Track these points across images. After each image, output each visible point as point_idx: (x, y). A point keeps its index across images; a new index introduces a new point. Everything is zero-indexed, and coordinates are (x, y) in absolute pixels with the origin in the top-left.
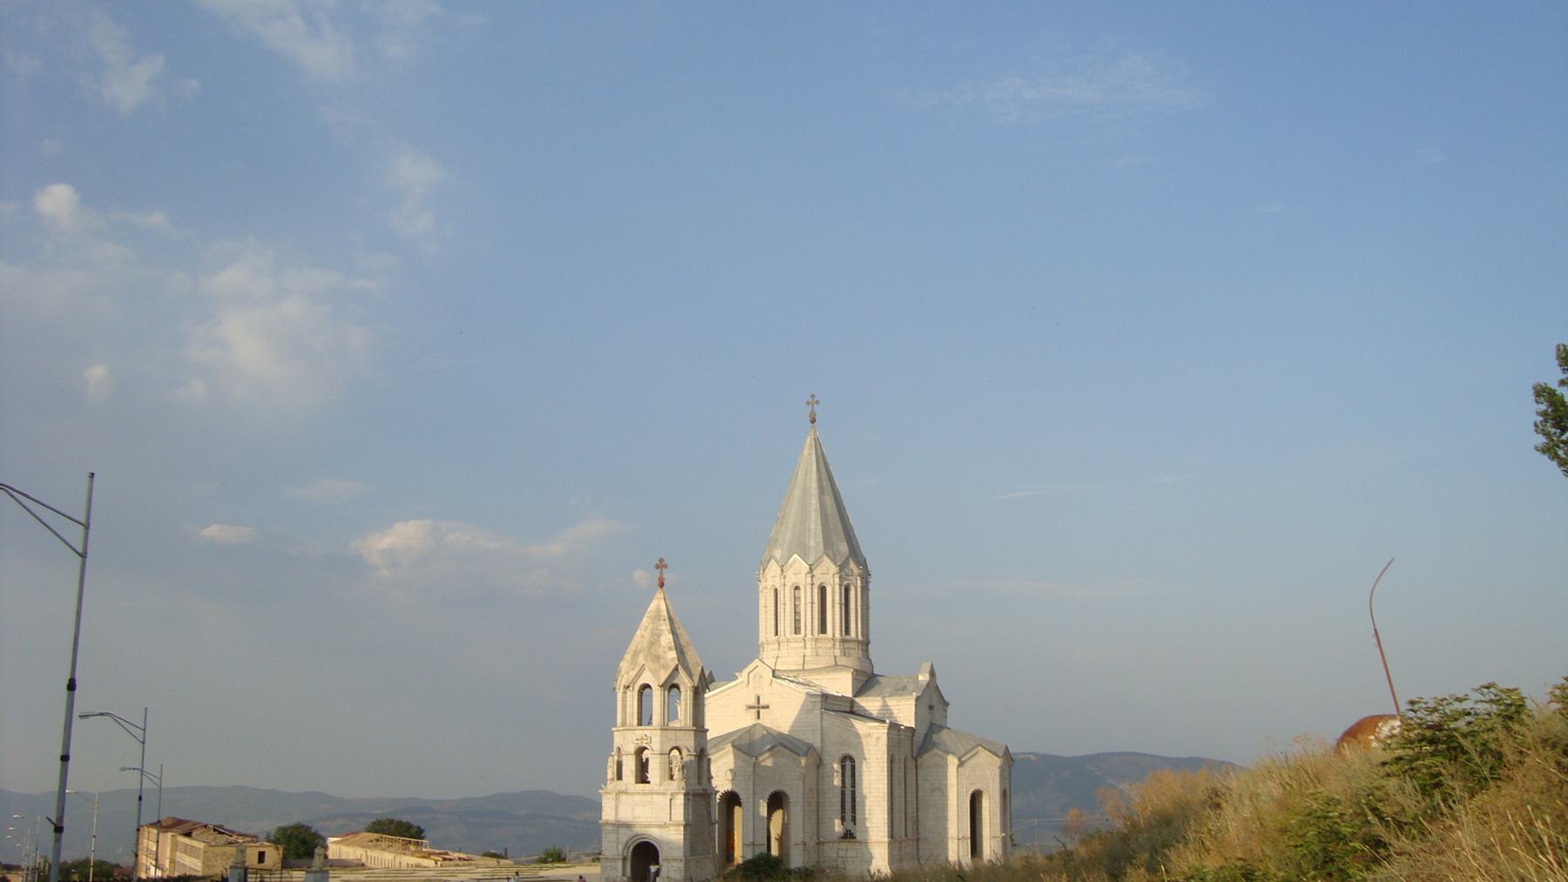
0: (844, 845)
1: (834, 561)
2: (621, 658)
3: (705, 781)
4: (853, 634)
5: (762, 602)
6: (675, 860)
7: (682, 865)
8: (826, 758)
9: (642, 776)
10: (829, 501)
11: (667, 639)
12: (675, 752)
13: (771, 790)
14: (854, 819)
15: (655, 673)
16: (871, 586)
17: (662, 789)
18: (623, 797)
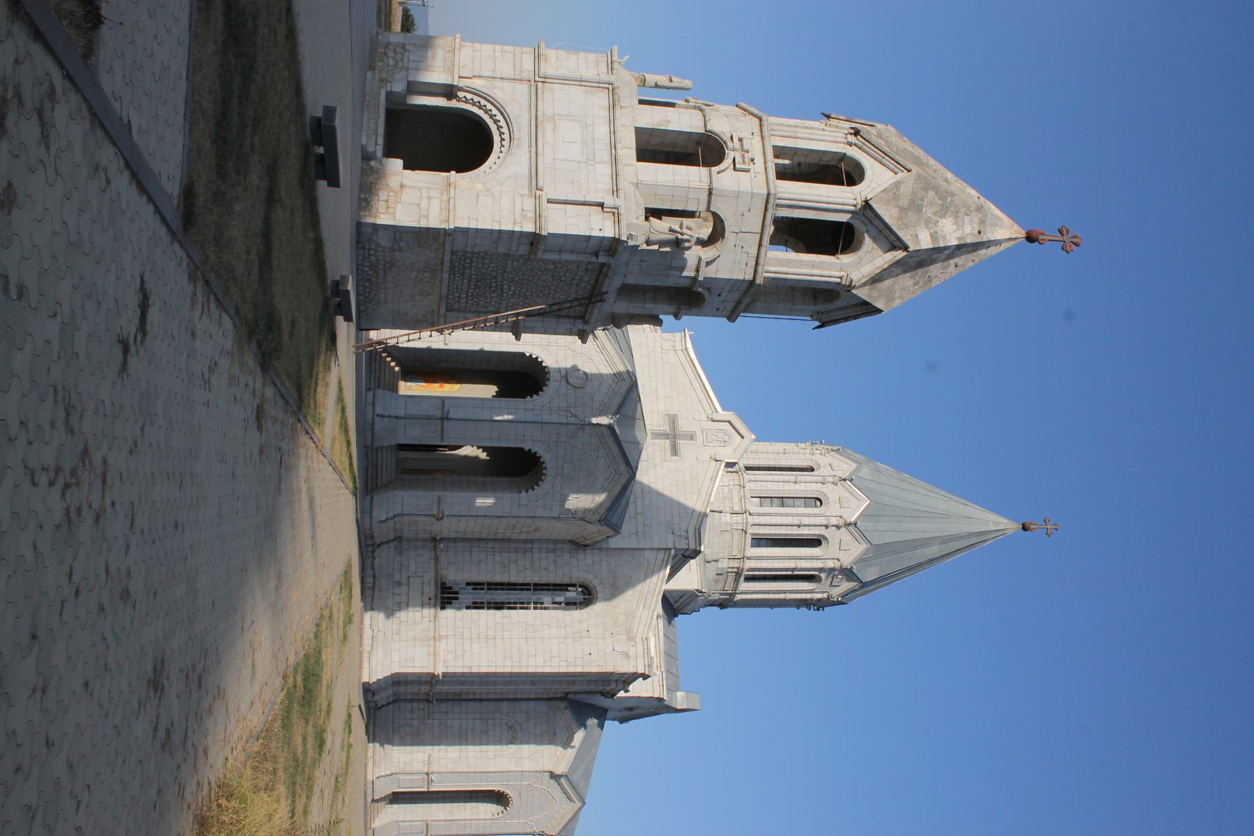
0: (430, 590)
1: (861, 560)
2: (903, 131)
3: (622, 307)
4: (744, 586)
5: (790, 447)
6: (448, 207)
7: (434, 221)
8: (588, 558)
9: (656, 148)
10: (933, 551)
11: (951, 233)
12: (705, 232)
13: (546, 456)
14: (477, 606)
15: (892, 192)
16: (804, 609)
18: (602, 99)
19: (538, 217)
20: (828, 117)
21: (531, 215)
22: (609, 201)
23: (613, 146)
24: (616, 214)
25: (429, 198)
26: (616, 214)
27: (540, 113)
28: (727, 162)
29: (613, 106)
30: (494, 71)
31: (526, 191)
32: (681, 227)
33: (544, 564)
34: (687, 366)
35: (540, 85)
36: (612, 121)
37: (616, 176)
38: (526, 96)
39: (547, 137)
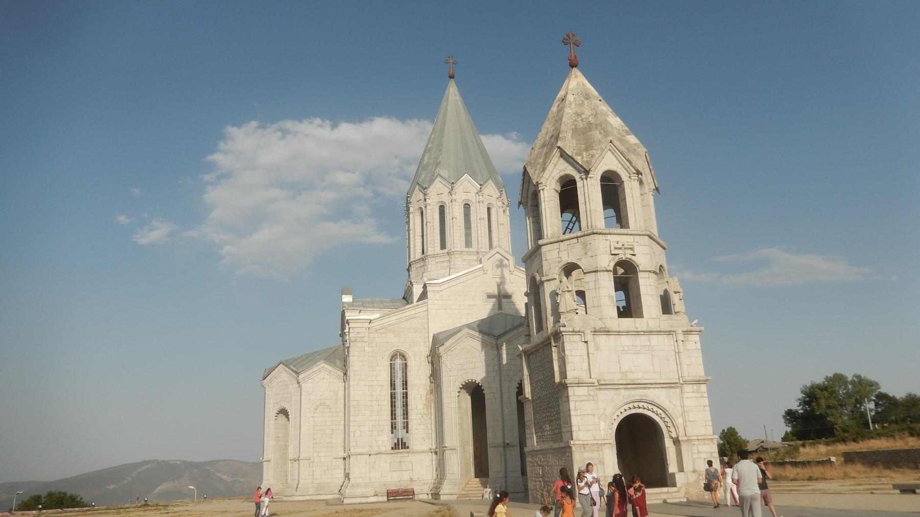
6: (703, 440)
18: (602, 339)
19: (698, 382)
21: (695, 387)
22: (681, 337)
23: (637, 333)
26: (687, 332)
27: (625, 382)
28: (633, 258)
30: (594, 415)
31: (678, 390)
32: (676, 293)
34: (451, 284)
35: (603, 382)
36: (619, 333)
37: (659, 332)
38: (607, 392)
39: (638, 376)
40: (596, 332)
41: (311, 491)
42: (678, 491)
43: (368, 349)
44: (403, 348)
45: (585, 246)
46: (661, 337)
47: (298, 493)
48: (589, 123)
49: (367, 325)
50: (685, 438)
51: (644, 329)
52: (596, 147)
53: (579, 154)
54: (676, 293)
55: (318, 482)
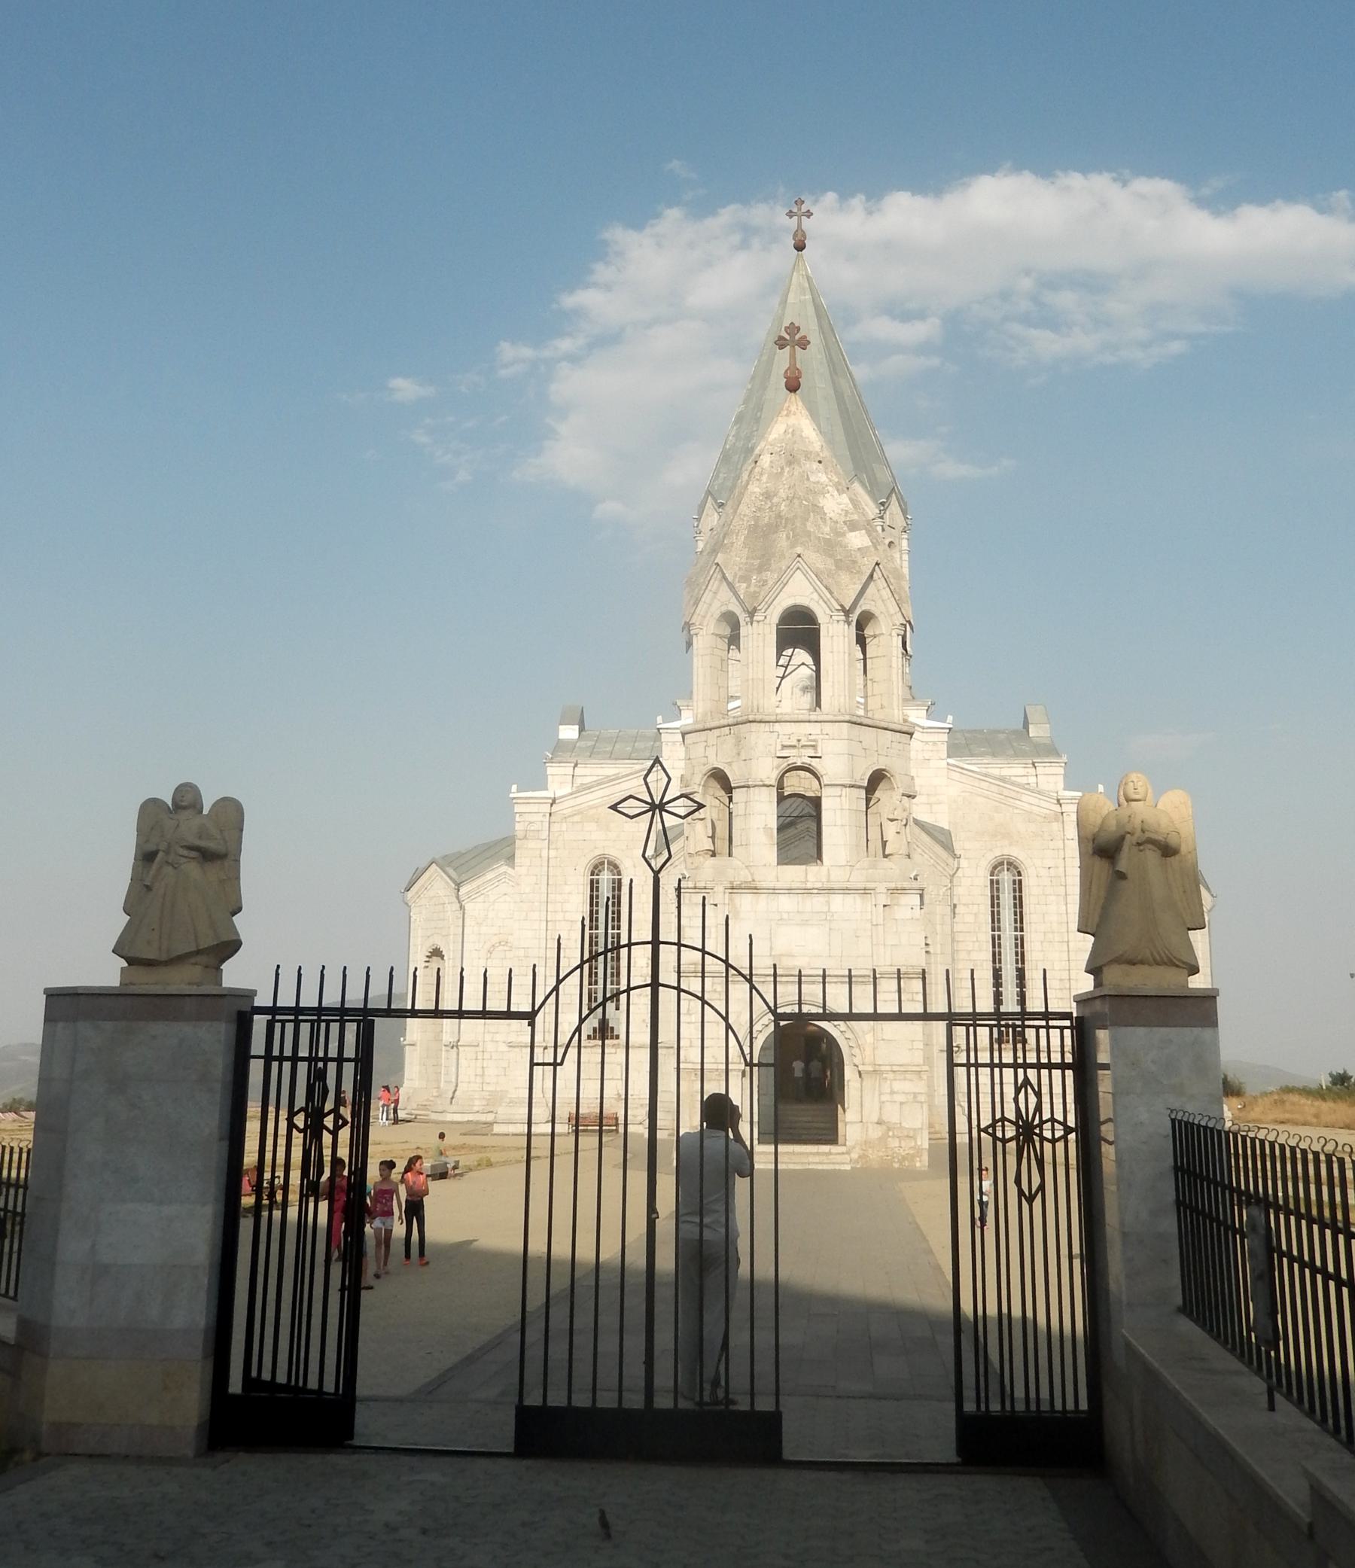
6: (902, 1072)
17: (858, 879)
20: (687, 626)
22: (883, 899)
24: (896, 891)
25: (892, 1093)
26: (896, 891)
29: (753, 889)
32: (892, 820)
33: (970, 919)
36: (774, 891)
37: (846, 891)
40: (733, 889)
41: (478, 1105)
42: (848, 1153)
43: (545, 853)
44: (613, 853)
45: (738, 741)
46: (849, 899)
47: (454, 1108)
48: (779, 516)
49: (546, 808)
50: (870, 1069)
51: (819, 885)
52: (773, 566)
53: (746, 579)
54: (892, 820)
55: (491, 1088)
